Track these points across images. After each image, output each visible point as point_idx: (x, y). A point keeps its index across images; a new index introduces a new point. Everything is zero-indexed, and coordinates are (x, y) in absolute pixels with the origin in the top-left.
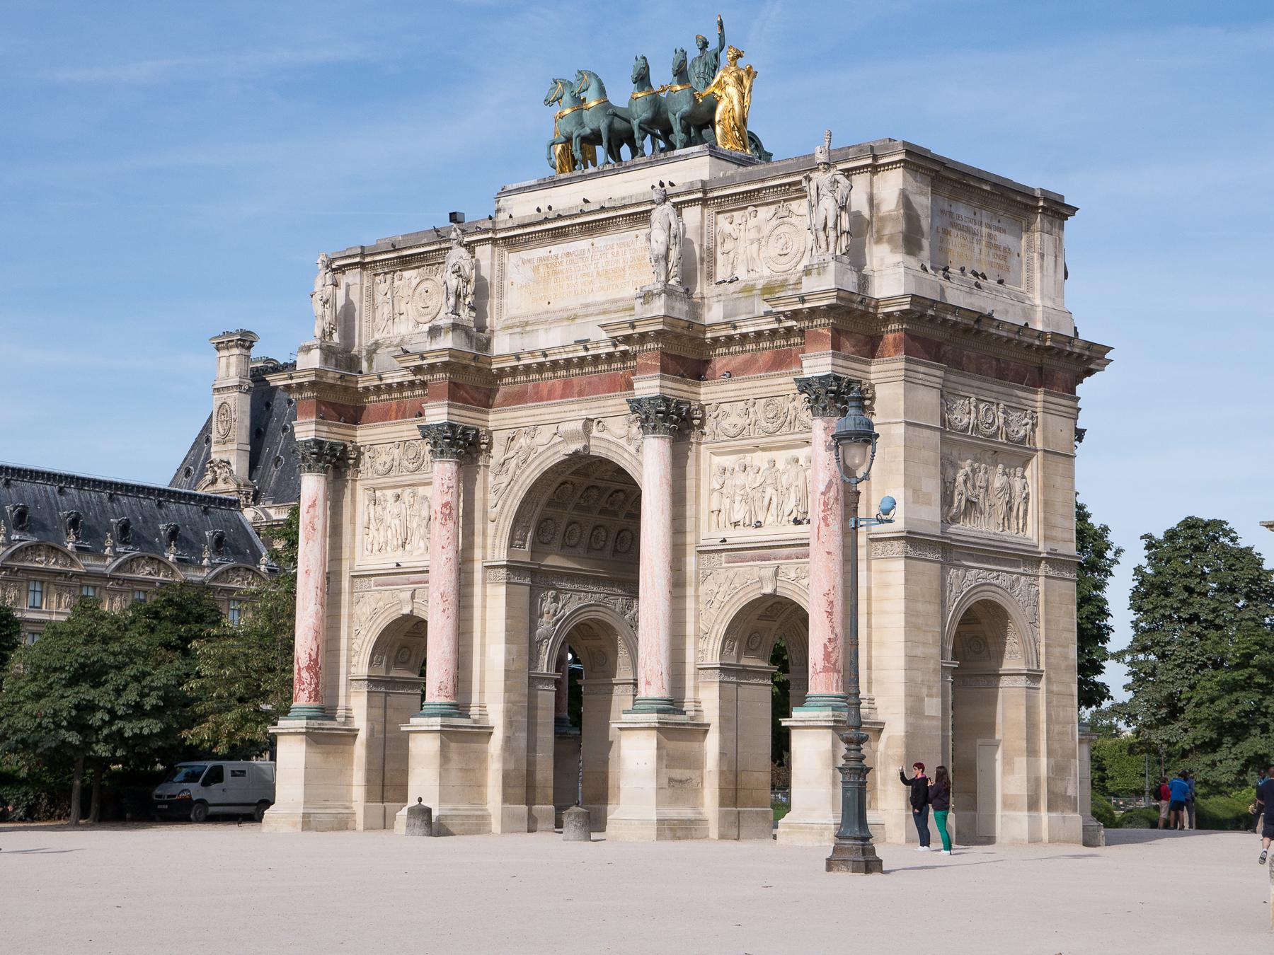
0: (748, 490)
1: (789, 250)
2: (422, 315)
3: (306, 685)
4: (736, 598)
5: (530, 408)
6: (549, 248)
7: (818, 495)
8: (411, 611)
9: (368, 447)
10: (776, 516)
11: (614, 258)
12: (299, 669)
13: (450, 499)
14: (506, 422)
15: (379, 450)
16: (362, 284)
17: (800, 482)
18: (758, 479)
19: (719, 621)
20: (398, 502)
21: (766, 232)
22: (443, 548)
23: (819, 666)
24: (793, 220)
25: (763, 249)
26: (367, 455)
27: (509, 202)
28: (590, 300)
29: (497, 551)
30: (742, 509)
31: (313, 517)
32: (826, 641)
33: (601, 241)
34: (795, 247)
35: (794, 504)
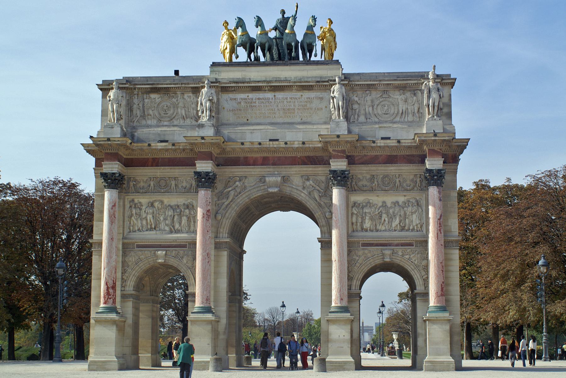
0: (372, 215)
3: (112, 296)
4: (368, 263)
6: (247, 95)
8: (165, 262)
9: (132, 179)
10: (387, 226)
11: (288, 104)
13: (210, 208)
14: (227, 173)
15: (139, 180)
16: (126, 98)
17: (402, 213)
18: (376, 211)
19: (359, 272)
20: (151, 207)
22: (208, 231)
23: (439, 294)
24: (391, 100)
25: (375, 110)
26: (131, 184)
29: (221, 235)
30: (369, 223)
32: (442, 283)
34: (392, 112)
35: (399, 222)
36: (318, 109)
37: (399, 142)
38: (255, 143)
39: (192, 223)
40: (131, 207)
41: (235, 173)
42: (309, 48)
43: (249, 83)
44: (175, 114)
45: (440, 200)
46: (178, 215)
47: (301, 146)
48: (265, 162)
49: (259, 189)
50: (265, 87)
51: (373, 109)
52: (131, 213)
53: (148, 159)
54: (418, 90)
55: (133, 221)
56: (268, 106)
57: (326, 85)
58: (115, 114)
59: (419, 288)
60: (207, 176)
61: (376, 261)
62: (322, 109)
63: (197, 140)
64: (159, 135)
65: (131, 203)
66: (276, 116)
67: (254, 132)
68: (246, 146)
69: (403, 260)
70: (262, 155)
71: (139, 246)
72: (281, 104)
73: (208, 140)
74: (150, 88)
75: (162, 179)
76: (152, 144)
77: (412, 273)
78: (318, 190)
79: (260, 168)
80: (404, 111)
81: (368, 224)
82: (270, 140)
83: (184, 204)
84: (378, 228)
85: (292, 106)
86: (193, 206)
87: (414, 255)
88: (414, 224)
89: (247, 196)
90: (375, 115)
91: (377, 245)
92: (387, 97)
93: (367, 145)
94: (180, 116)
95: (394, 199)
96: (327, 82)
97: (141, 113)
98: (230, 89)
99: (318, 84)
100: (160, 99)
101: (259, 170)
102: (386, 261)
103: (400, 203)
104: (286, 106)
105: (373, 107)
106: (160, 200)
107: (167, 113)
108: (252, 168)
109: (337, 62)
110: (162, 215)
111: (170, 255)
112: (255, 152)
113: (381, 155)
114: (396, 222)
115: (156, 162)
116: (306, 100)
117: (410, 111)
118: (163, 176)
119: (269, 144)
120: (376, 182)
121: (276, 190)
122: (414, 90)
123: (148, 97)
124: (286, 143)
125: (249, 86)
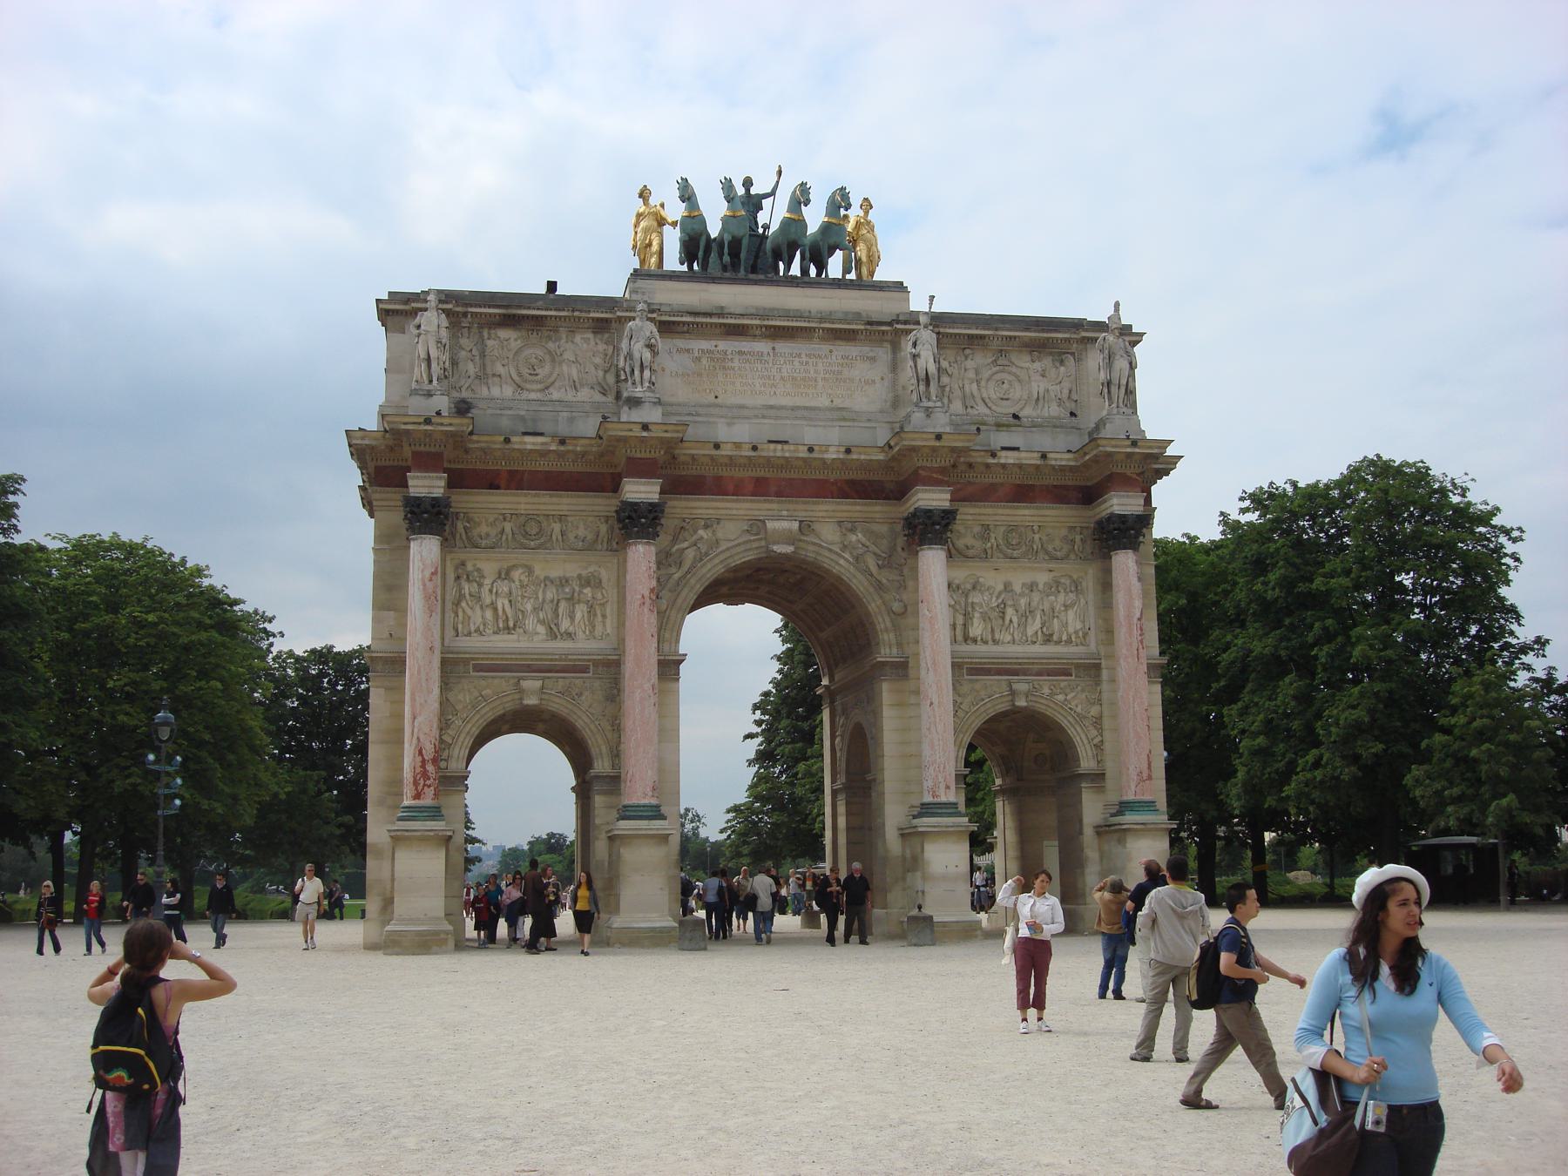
0: (986, 609)
1: (1010, 396)
2: (526, 381)
4: (982, 709)
5: (713, 500)
7: (1135, 620)
12: (424, 762)
15: (477, 520)
17: (1046, 606)
18: (994, 599)
19: (964, 730)
21: (986, 374)
23: (1145, 775)
24: (1014, 370)
25: (983, 390)
26: (460, 525)
28: (772, 402)
31: (436, 587)
33: (784, 347)
36: (867, 382)
37: (1044, 456)
38: (744, 445)
39: (599, 618)
40: (458, 578)
41: (700, 511)
42: (818, 257)
44: (555, 375)
45: (1140, 579)
46: (566, 599)
47: (841, 456)
48: (760, 488)
49: (748, 546)
52: (460, 592)
53: (497, 473)
54: (1065, 353)
55: (464, 611)
57: (883, 332)
58: (434, 365)
59: (1086, 763)
60: (650, 511)
61: (997, 707)
63: (631, 430)
64: (522, 419)
65: (460, 571)
67: (734, 424)
68: (724, 453)
69: (1052, 705)
70: (754, 474)
71: (479, 668)
73: (656, 432)
74: (500, 315)
75: (530, 518)
76: (514, 439)
77: (1071, 731)
78: (875, 554)
79: (751, 501)
80: (1041, 395)
81: (977, 629)
82: (770, 442)
83: (580, 577)
84: (997, 637)
85: (812, 372)
86: (601, 582)
87: (1073, 694)
88: (1071, 630)
89: (721, 562)
90: (984, 401)
91: (999, 672)
92: (1006, 363)
93: (979, 460)
94: (567, 382)
95: (1028, 577)
96: (890, 324)
97: (477, 370)
98: (680, 328)
99: (869, 327)
100: (519, 342)
101: (747, 505)
102: (1021, 708)
103: (1041, 587)
105: (978, 382)
106: (526, 566)
107: (537, 371)
108: (733, 501)
109: (899, 287)
110: (530, 598)
111: (552, 690)
112: (740, 466)
113: (1002, 484)
114: (1034, 626)
115: (517, 480)
116: (841, 361)
117: (1052, 394)
118: (531, 512)
119: (775, 450)
120: (993, 540)
121: (789, 549)
122: (1061, 354)
123: (493, 336)
124: (811, 450)
125: (721, 324)
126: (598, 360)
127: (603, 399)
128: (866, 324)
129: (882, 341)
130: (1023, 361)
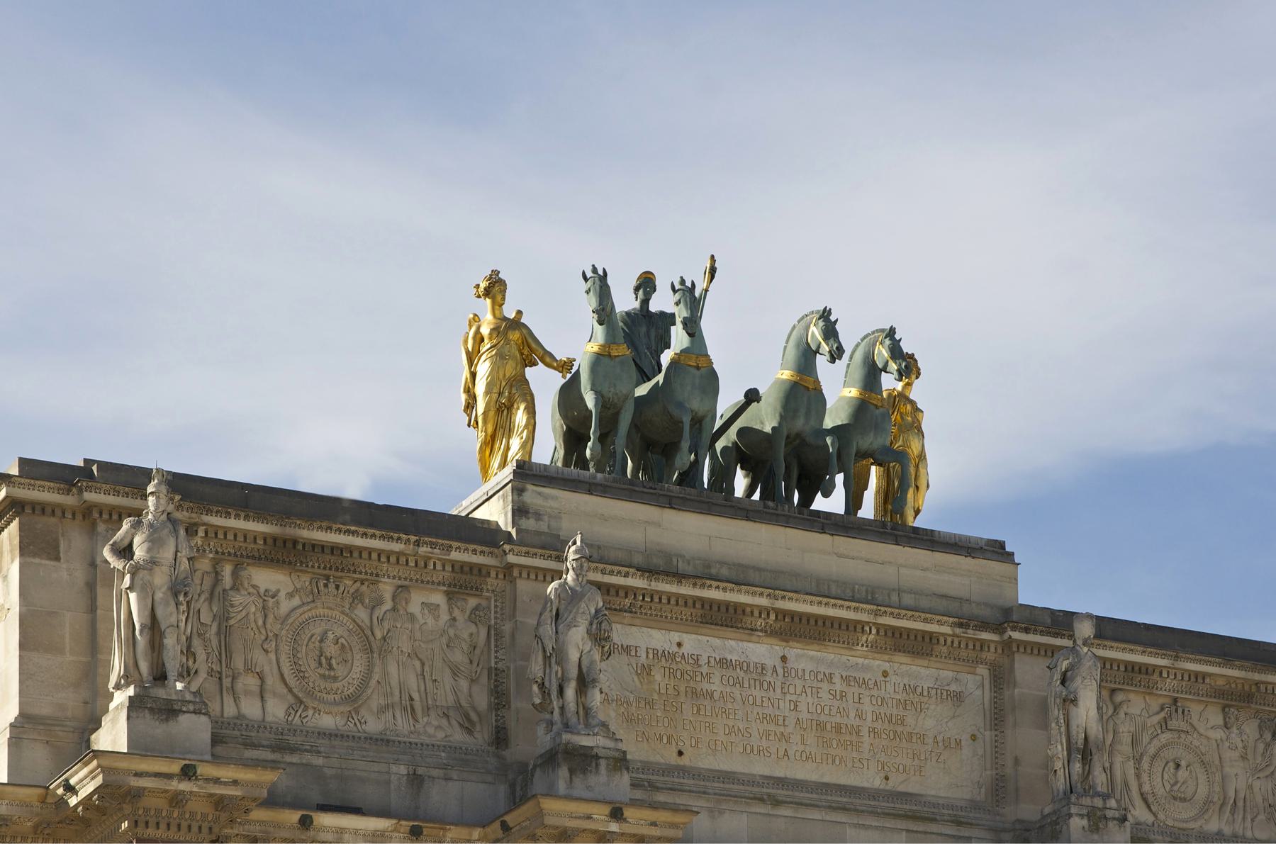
6: (676, 637)
11: (836, 703)
25: (1145, 777)
27: (551, 503)
28: (779, 773)
33: (804, 656)
34: (1203, 791)
43: (703, 586)
50: (756, 613)
51: (1138, 776)
56: (759, 701)
57: (983, 644)
62: (959, 743)
66: (791, 753)
72: (810, 700)
80: (1241, 795)
85: (852, 714)
92: (1184, 726)
94: (397, 698)
99: (958, 631)
100: (296, 601)
104: (827, 711)
105: (1138, 762)
107: (340, 671)
125: (696, 600)
126: (459, 657)
127: (468, 739)
128: (953, 625)
129: (977, 661)
130: (1207, 719)
